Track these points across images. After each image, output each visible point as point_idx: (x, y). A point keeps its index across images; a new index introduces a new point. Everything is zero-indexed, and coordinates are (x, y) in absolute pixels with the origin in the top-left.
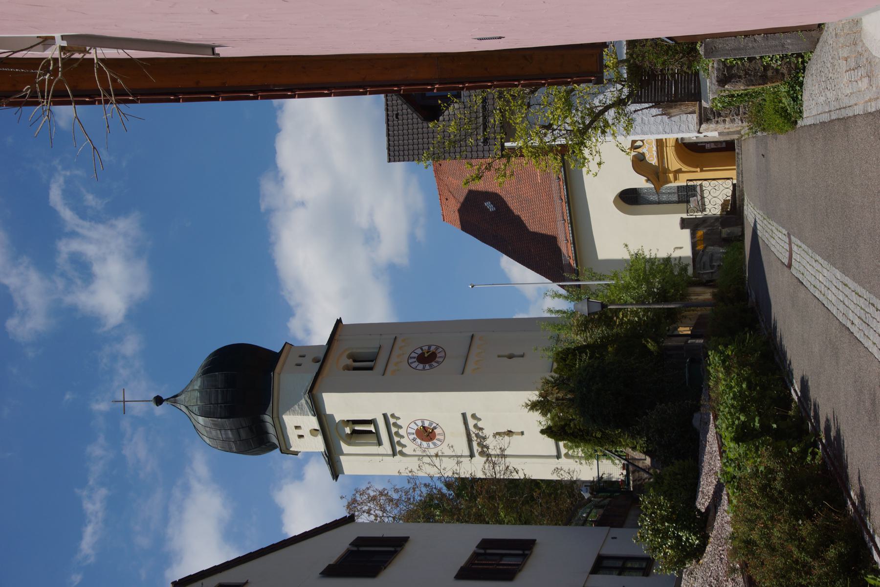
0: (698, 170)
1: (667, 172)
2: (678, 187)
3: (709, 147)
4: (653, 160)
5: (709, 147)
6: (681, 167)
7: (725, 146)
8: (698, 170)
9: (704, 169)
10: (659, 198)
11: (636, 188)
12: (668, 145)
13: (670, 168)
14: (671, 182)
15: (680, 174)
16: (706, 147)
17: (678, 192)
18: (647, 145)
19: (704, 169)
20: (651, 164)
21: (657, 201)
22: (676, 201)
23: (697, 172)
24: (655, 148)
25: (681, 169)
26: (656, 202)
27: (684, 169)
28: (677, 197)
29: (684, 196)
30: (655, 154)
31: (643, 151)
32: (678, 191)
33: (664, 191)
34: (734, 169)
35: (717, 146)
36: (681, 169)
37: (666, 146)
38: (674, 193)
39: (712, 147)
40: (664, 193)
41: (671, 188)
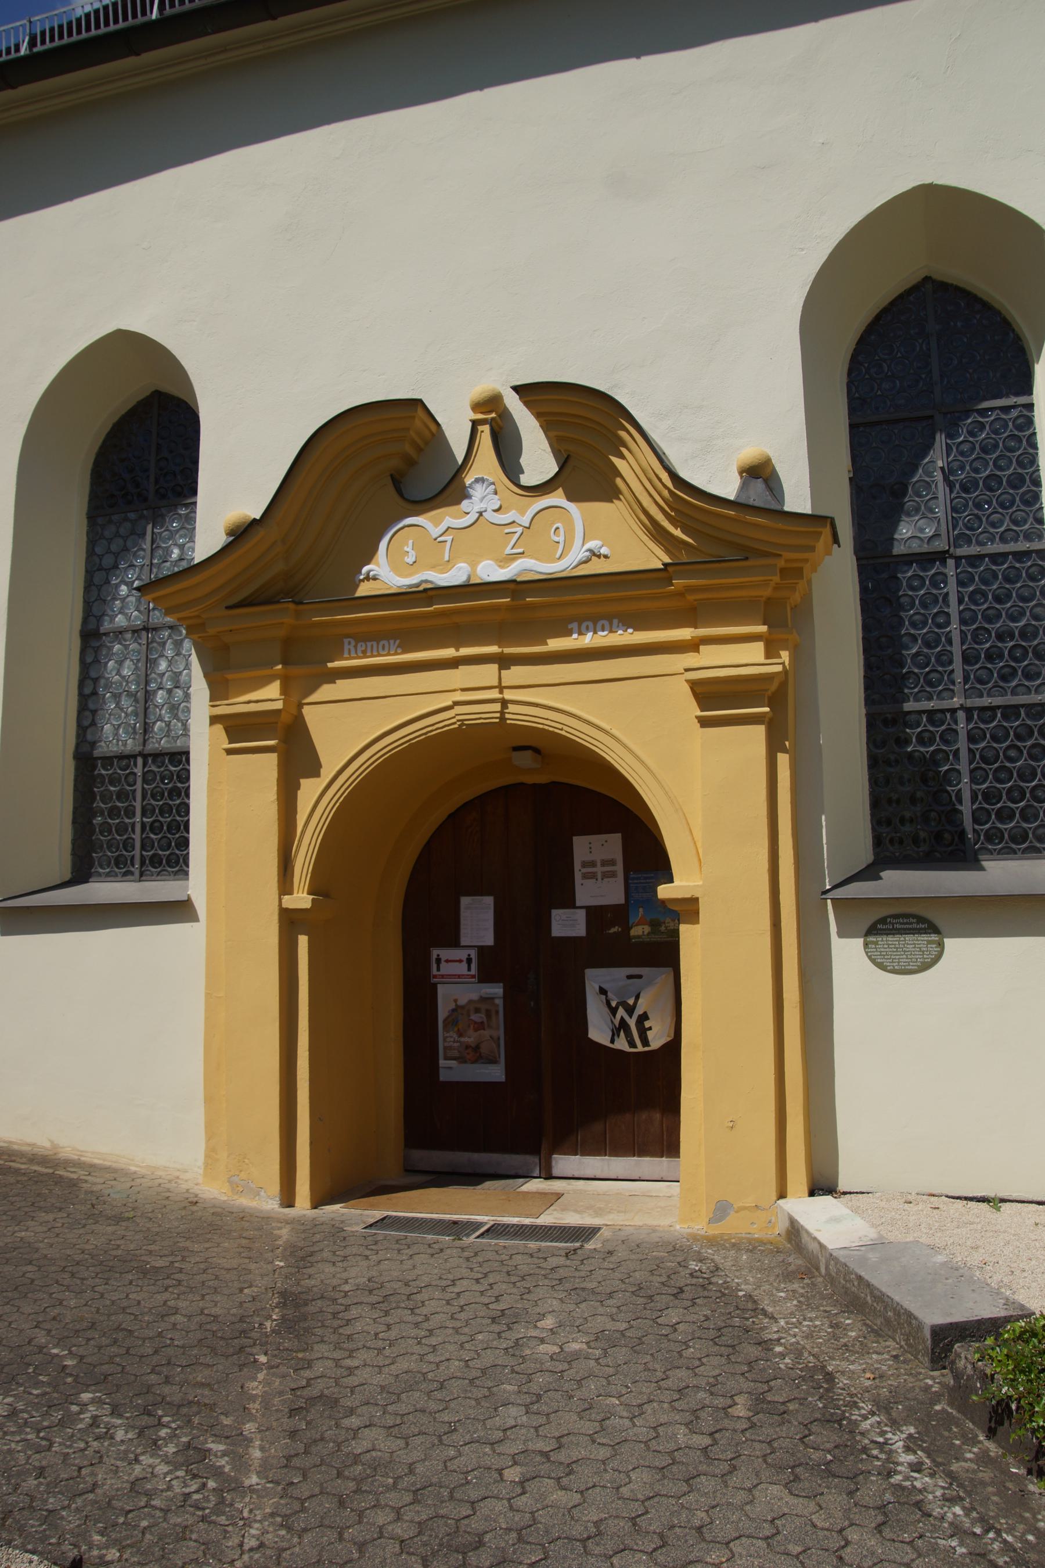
0: (301, 899)
1: (296, 670)
2: (181, 757)
3: (446, 969)
4: (397, 567)
5: (446, 969)
6: (328, 772)
7: (444, 1076)
8: (301, 899)
9: (303, 941)
10: (120, 633)
11: (194, 492)
12: (516, 674)
13: (326, 691)
14: (218, 691)
15: (273, 758)
16: (445, 953)
17: (145, 757)
18: (525, 520)
19: (303, 941)
20: (369, 555)
21: (106, 626)
22: (93, 744)
23: (285, 885)
24: (490, 571)
25: (314, 769)
26: (99, 619)
27: (309, 790)
28: (114, 749)
29: (122, 795)
30: (455, 576)
31: (478, 492)
32: (157, 756)
33: (163, 665)
34: (288, 1199)
35: (452, 1021)
36: (314, 769)
37: (504, 662)
38: (147, 728)
39: (441, 989)
40: (151, 663)
41: (179, 710)
